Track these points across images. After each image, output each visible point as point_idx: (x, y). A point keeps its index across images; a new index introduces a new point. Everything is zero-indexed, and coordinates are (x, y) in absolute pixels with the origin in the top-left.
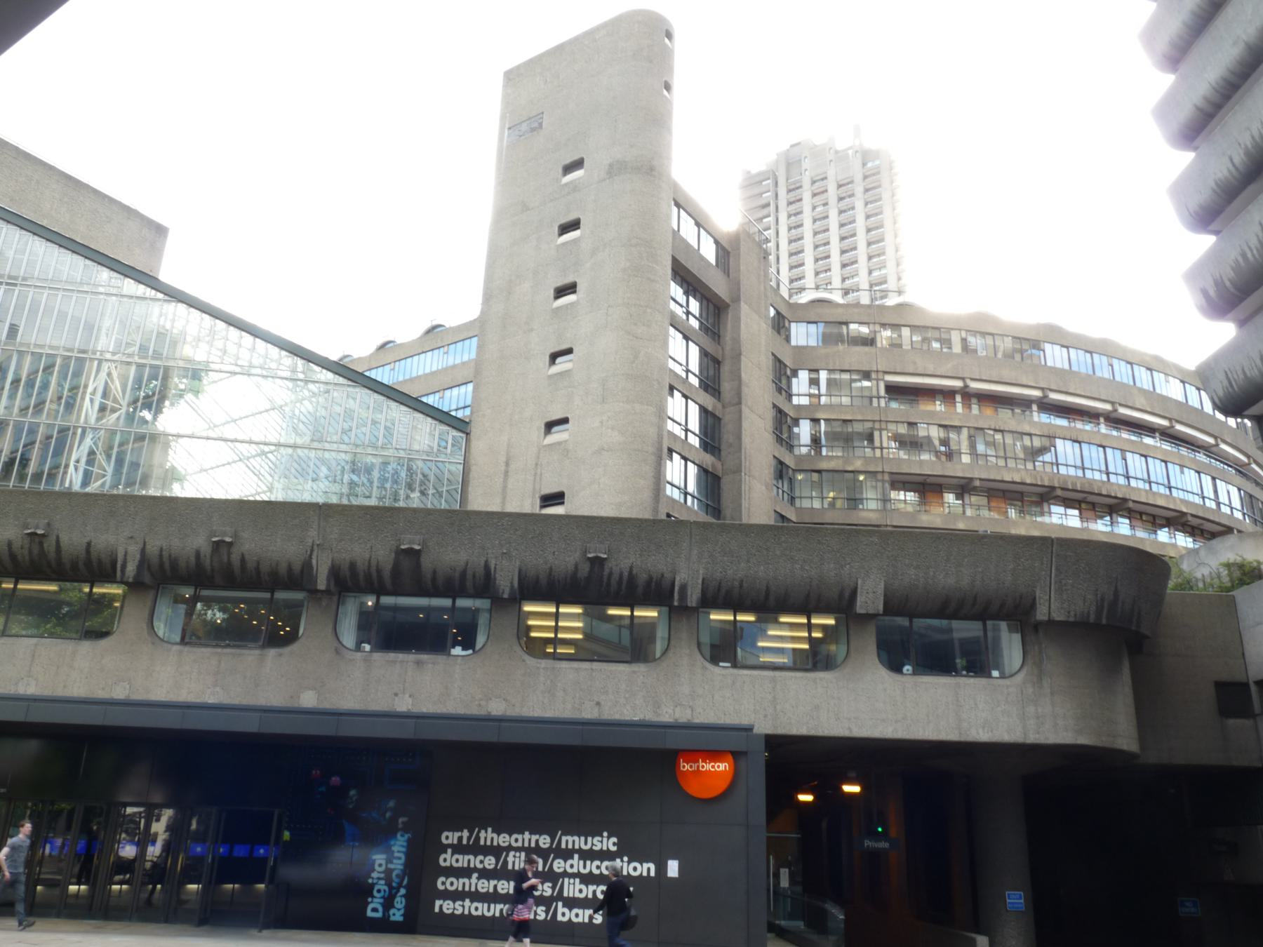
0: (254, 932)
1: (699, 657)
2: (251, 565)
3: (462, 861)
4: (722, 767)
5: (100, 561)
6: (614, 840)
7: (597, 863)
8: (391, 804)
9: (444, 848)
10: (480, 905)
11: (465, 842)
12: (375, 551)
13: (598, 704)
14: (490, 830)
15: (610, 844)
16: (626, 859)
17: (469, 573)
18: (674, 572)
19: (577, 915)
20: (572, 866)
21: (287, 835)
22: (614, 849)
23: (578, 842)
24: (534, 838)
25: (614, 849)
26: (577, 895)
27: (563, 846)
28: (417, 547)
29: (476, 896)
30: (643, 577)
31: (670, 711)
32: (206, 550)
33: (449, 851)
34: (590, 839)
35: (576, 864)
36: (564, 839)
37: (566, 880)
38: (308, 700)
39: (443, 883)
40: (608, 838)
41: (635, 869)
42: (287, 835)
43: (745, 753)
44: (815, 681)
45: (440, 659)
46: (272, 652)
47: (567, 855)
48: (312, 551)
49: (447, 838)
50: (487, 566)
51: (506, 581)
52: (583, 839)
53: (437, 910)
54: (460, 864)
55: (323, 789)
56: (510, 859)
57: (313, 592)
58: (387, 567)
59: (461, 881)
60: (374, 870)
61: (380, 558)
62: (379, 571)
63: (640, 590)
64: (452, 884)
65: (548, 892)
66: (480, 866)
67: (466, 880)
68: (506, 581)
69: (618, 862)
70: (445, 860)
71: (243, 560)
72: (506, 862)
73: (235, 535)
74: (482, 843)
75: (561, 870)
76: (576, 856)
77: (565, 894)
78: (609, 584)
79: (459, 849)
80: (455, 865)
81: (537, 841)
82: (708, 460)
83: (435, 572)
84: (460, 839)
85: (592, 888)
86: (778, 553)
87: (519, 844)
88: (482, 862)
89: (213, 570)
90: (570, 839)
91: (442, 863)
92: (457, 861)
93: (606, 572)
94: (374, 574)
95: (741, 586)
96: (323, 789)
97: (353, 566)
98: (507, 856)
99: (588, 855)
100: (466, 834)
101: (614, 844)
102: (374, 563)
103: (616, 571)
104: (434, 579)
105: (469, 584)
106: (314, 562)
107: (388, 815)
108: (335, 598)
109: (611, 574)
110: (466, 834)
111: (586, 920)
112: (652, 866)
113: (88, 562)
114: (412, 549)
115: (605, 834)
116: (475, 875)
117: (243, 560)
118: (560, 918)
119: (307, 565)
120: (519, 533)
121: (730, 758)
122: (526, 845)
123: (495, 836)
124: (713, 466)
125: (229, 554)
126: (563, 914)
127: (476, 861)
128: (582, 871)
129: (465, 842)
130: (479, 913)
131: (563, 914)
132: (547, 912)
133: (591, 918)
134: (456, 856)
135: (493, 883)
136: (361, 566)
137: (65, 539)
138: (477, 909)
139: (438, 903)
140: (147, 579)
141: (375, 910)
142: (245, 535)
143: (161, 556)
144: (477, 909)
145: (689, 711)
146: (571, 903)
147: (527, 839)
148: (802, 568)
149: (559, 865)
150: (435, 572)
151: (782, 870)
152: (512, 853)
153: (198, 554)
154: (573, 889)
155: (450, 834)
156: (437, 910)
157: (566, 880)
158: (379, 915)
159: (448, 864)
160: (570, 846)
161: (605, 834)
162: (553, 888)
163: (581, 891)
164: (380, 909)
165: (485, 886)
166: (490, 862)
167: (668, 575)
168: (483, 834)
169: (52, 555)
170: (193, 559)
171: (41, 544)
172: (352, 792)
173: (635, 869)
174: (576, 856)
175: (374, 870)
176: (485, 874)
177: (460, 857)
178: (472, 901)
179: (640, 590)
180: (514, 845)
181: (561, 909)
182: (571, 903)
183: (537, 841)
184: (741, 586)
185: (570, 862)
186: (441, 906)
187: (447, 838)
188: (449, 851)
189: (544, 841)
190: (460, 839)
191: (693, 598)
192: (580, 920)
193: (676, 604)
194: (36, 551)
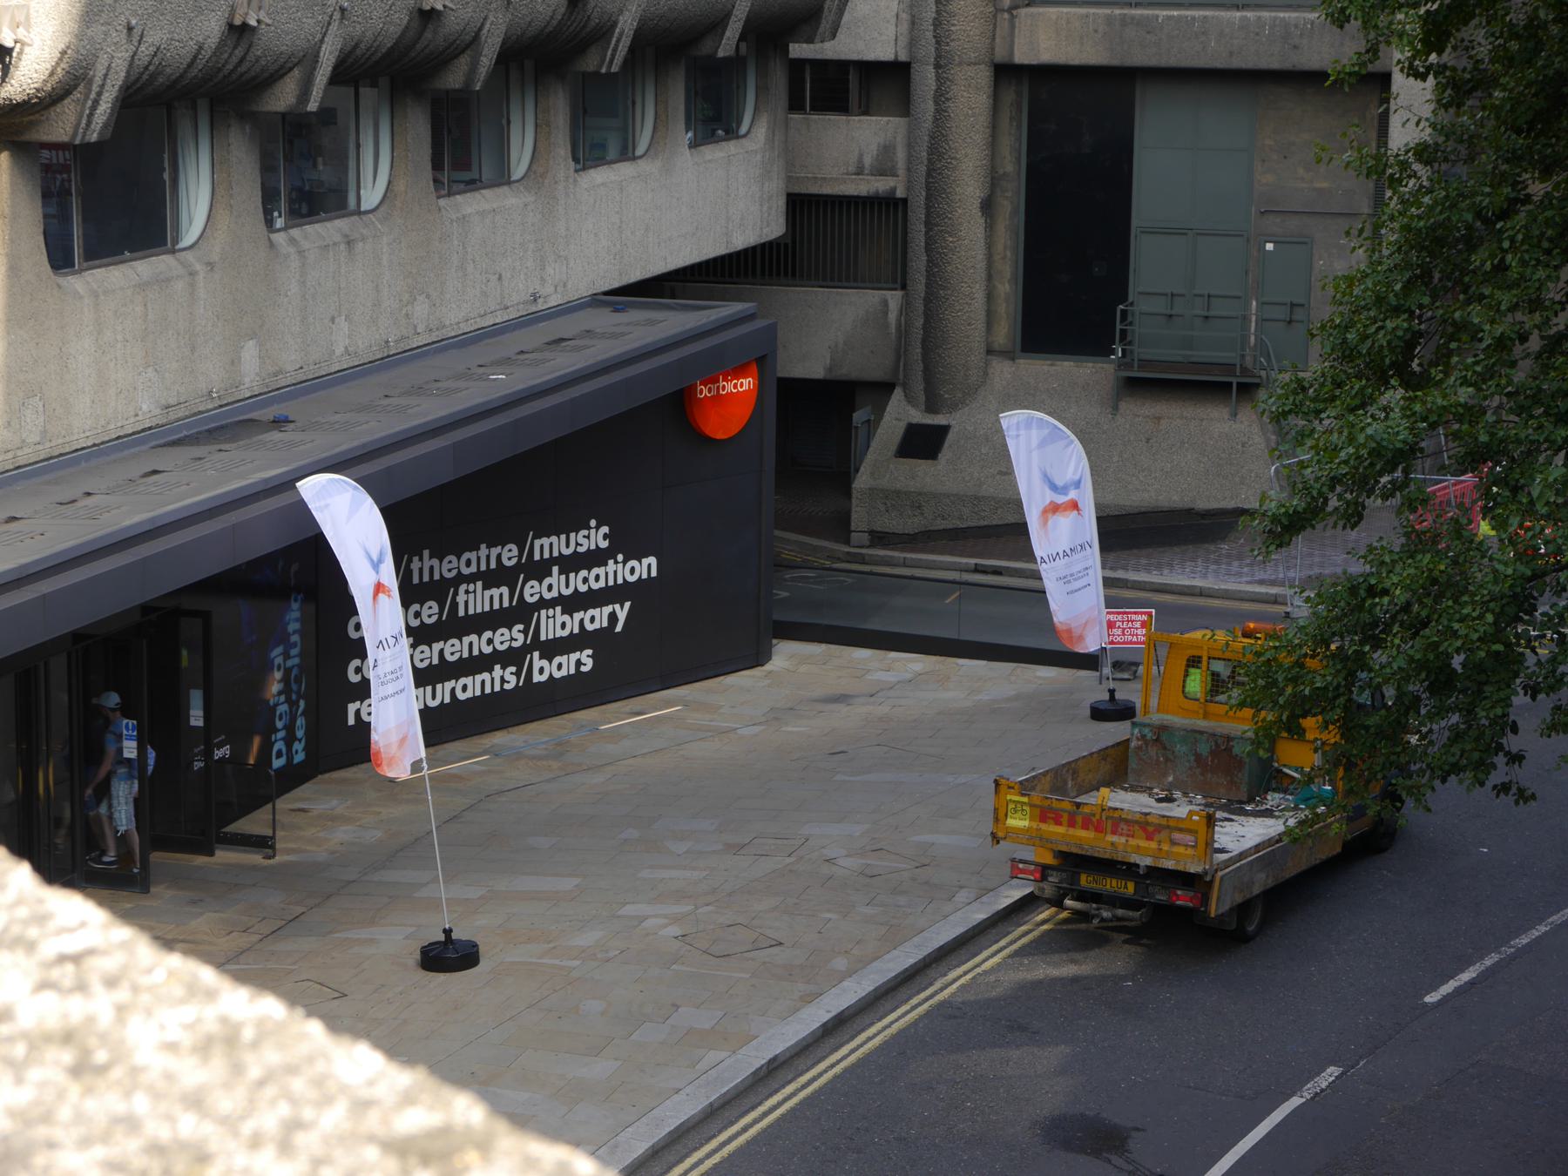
14: (426, 553)
22: (604, 544)
24: (495, 551)
25: (604, 544)
26: (560, 633)
35: (557, 584)
36: (537, 543)
40: (597, 528)
43: (764, 357)
47: (539, 570)
53: (351, 721)
56: (461, 599)
72: (455, 605)
81: (499, 557)
87: (473, 569)
90: (545, 541)
98: (456, 593)
99: (570, 564)
101: (605, 537)
112: (652, 560)
123: (435, 562)
135: (437, 646)
149: (532, 591)
152: (463, 588)
154: (554, 625)
156: (351, 721)
160: (546, 555)
161: (593, 523)
174: (555, 569)
182: (552, 649)
186: (358, 712)
189: (509, 555)
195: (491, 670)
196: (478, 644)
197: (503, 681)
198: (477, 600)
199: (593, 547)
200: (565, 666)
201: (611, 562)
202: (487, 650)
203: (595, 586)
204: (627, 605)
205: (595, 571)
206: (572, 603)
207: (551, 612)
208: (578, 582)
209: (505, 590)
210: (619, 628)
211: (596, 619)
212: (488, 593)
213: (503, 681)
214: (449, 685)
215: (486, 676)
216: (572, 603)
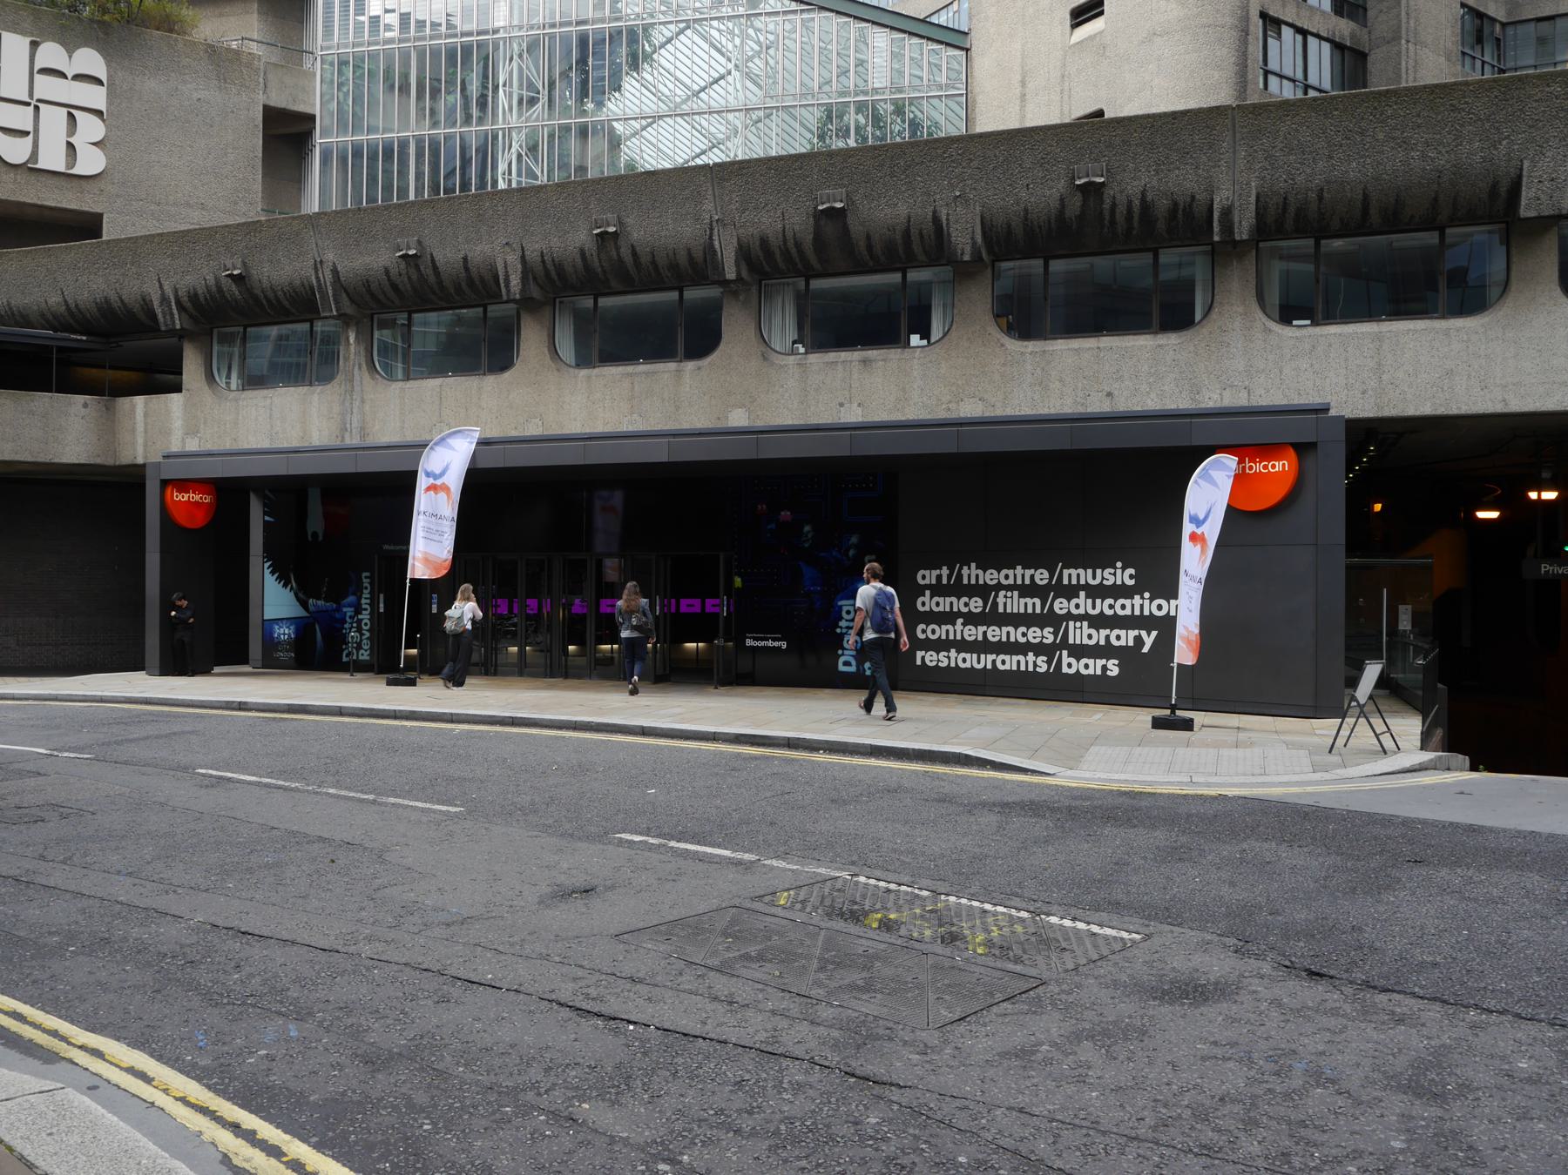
0: (711, 690)
1: (1260, 314)
2: (645, 259)
3: (944, 604)
4: (1279, 466)
5: (482, 280)
6: (1132, 571)
7: (1110, 601)
8: (854, 540)
9: (920, 590)
10: (968, 656)
11: (945, 581)
12: (783, 218)
13: (1109, 394)
14: (973, 565)
15: (1126, 577)
16: (1147, 595)
17: (914, 232)
18: (1211, 191)
19: (1086, 666)
20: (1077, 606)
21: (738, 582)
23: (1085, 576)
24: (1029, 573)
25: (1132, 582)
26: (1086, 641)
27: (1065, 582)
28: (839, 205)
29: (963, 646)
30: (1163, 205)
31: (1216, 397)
32: (590, 246)
33: (928, 593)
34: (1099, 571)
36: (1066, 572)
37: (1071, 623)
38: (738, 419)
39: (924, 631)
40: (1123, 569)
41: (1160, 607)
42: (738, 582)
43: (1312, 446)
44: (1447, 333)
45: (893, 354)
46: (690, 365)
47: (1070, 592)
48: (711, 229)
49: (924, 577)
50: (936, 219)
51: (964, 236)
52: (1090, 571)
53: (919, 662)
54: (941, 609)
55: (773, 526)
56: (1001, 600)
57: (724, 283)
58: (809, 238)
59: (944, 628)
60: (841, 618)
61: (797, 228)
62: (798, 245)
63: (1161, 226)
64: (933, 632)
65: (1050, 639)
66: (965, 610)
67: (950, 627)
68: (964, 236)
69: (1137, 600)
70: (923, 604)
71: (634, 254)
72: (995, 604)
73: (621, 223)
74: (965, 581)
75: (1064, 611)
76: (1082, 594)
77: (1071, 641)
78: (1113, 222)
79: (938, 590)
80: (935, 609)
81: (1032, 577)
82: (1344, 28)
83: (868, 237)
84: (939, 577)
85: (1104, 633)
86: (1381, 136)
87: (1010, 581)
88: (966, 605)
89: (604, 272)
90: (1074, 572)
91: (921, 609)
92: (938, 604)
93: (1106, 206)
94: (794, 251)
95: (1320, 198)
96: (773, 526)
97: (764, 241)
98: (996, 596)
99: (1097, 592)
100: (945, 571)
101: (1131, 577)
102: (789, 235)
103: (1121, 200)
104: (870, 247)
105: (916, 247)
106: (716, 243)
107: (851, 553)
108: (754, 289)
109: (1114, 206)
110: (945, 571)
111: (1099, 672)
113: (470, 281)
114: (833, 208)
115: (1119, 564)
116: (960, 621)
117: (634, 254)
118: (1065, 670)
119: (709, 249)
120: (975, 164)
121: (1292, 453)
122: (1019, 582)
123: (980, 572)
124: (1353, 36)
125: (618, 248)
126: (1070, 665)
127: (959, 604)
128: (1091, 611)
129: (945, 581)
130: (968, 665)
131: (1070, 665)
132: (1049, 663)
133: (1104, 668)
134: (936, 599)
135: (982, 629)
136: (775, 242)
137: (440, 258)
138: (964, 660)
139: (919, 654)
140: (536, 293)
141: (847, 664)
142: (630, 221)
143: (543, 262)
144: (964, 660)
145: (1244, 394)
146: (1079, 652)
147: (1020, 574)
148: (1424, 157)
149: (1061, 606)
150: (868, 237)
151: (1402, 608)
152: (1002, 593)
153: (582, 252)
154: (1080, 634)
155: (927, 573)
156: (919, 662)
157: (1071, 623)
158: (853, 669)
159: (927, 608)
160: (1074, 582)
161: (1119, 564)
162: (1055, 634)
163: (1090, 637)
164: (854, 663)
165: (972, 633)
166: (976, 605)
167: (1201, 197)
168: (965, 571)
169: (432, 279)
170: (579, 261)
171: (417, 266)
172: (807, 528)
173: (1160, 607)
174: (1082, 594)
175: (841, 618)
176: (971, 619)
177: (941, 600)
178: (958, 652)
179: (1161, 226)
180: (1004, 582)
181: (1066, 659)
182: (1079, 652)
183: (1032, 577)
184: (1320, 198)
185: (1074, 601)
187: (924, 577)
188: (928, 593)
189: (1041, 577)
190: (939, 577)
191: (1244, 227)
192: (1091, 671)
193: (1216, 238)
194: (415, 277)
195: (1025, 655)
196: (1017, 634)
197: (1035, 665)
198: (1013, 603)
199: (1119, 582)
200: (1093, 667)
201: (1137, 597)
202: (1023, 640)
203: (1121, 613)
204: (1154, 633)
205: (1121, 601)
206: (1098, 622)
207: (1078, 624)
208: (1104, 606)
209: (1037, 601)
210: (1145, 650)
211: (1126, 638)
212: (1023, 601)
213: (1035, 665)
214: (991, 657)
215: (1021, 658)
216: (1098, 622)
